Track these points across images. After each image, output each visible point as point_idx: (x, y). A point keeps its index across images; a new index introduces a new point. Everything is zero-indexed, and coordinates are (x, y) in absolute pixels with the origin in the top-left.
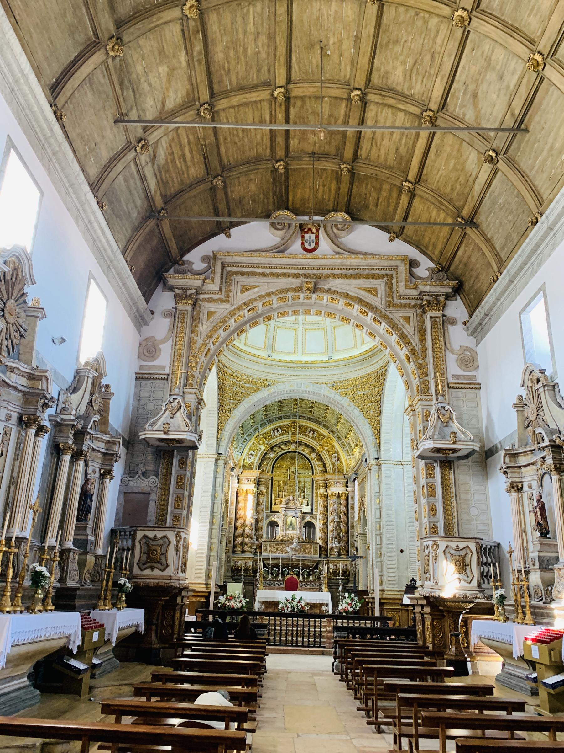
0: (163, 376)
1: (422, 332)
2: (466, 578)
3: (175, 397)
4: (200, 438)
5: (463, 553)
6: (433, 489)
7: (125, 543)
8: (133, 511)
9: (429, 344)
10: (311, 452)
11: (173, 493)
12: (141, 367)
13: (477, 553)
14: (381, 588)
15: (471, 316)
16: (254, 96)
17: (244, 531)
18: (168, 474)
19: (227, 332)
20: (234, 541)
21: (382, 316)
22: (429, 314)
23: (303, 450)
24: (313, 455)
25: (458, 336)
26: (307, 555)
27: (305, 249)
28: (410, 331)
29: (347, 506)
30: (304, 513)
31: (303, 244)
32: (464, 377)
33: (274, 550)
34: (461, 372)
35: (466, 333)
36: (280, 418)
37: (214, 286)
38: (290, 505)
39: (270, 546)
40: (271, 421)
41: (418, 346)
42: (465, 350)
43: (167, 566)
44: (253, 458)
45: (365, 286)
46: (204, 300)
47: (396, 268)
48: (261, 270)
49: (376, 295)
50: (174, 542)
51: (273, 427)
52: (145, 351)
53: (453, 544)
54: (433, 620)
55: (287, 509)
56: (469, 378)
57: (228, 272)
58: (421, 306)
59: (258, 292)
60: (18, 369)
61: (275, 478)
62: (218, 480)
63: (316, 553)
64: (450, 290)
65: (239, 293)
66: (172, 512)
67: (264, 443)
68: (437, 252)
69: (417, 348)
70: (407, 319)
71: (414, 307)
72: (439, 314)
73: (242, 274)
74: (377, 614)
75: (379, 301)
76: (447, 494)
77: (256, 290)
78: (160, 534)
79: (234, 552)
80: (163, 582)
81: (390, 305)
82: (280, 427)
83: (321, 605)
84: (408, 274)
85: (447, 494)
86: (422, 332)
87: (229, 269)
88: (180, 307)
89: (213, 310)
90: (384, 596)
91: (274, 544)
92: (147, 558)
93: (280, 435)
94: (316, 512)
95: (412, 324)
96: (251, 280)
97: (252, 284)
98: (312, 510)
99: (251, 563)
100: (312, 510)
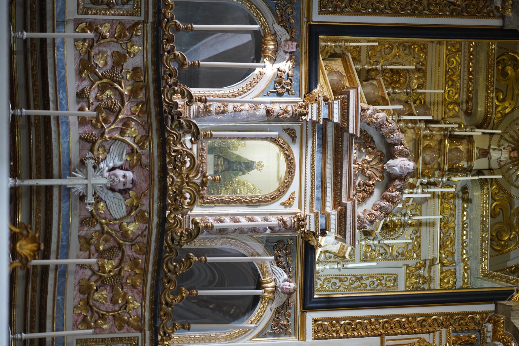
26: (72, 296)
30: (309, 250)
33: (102, 63)
38: (358, 157)
39: (125, 33)
55: (335, 139)
98: (330, 303)
100: (330, 303)
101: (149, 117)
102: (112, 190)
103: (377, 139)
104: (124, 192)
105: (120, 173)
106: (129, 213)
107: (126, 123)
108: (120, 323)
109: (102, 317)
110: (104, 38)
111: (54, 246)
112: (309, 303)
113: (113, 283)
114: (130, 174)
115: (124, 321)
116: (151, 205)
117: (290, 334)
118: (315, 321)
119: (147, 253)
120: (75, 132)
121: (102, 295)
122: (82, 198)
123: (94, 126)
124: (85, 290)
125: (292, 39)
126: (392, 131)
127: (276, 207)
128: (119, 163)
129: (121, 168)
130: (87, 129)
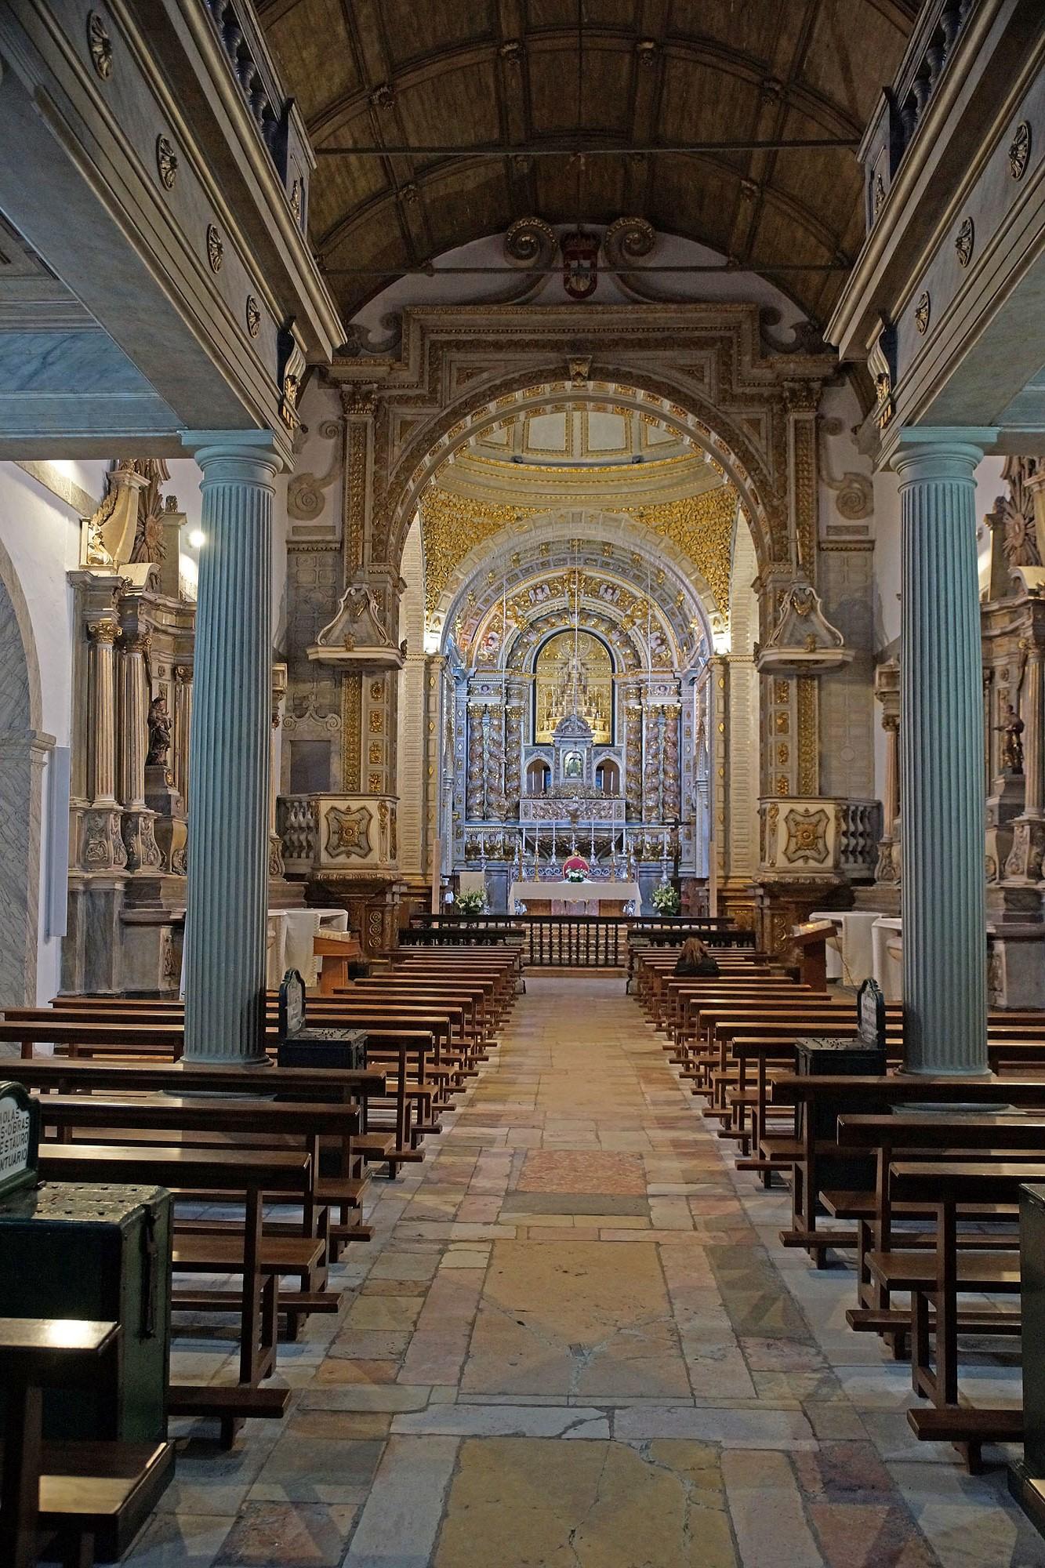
0: (333, 546)
1: (780, 448)
2: (816, 855)
3: (357, 586)
4: (403, 652)
5: (814, 820)
6: (785, 721)
7: (301, 817)
8: (307, 772)
9: (791, 470)
11: (367, 740)
12: (296, 530)
13: (837, 818)
14: (721, 873)
15: (865, 417)
16: (465, 59)
18: (355, 711)
19: (436, 456)
21: (710, 419)
22: (792, 417)
23: (594, 626)
25: (841, 454)
27: (572, 292)
28: (760, 445)
31: (567, 281)
32: (848, 530)
34: (843, 521)
35: (855, 448)
36: (545, 565)
37: (409, 375)
40: (528, 572)
41: (772, 478)
42: (851, 481)
43: (370, 850)
44: (495, 645)
45: (682, 362)
46: (391, 400)
47: (737, 328)
48: (491, 337)
49: (701, 380)
50: (377, 816)
51: (532, 582)
52: (299, 501)
53: (800, 807)
54: (773, 916)
56: (857, 530)
57: (433, 344)
58: (781, 399)
59: (489, 380)
60: (165, 606)
61: (541, 680)
62: (432, 699)
63: (619, 816)
64: (831, 371)
65: (454, 384)
66: (366, 767)
67: (516, 617)
68: (811, 295)
69: (771, 480)
70: (755, 424)
71: (767, 400)
72: (811, 416)
73: (459, 345)
74: (714, 914)
75: (705, 390)
76: (806, 729)
77: (485, 375)
78: (355, 805)
80: (368, 874)
81: (727, 397)
82: (546, 582)
83: (623, 903)
84: (758, 339)
85: (806, 729)
86: (780, 448)
87: (434, 337)
88: (352, 417)
89: (409, 418)
90: (730, 886)
91: (541, 803)
92: (340, 839)
93: (547, 598)
95: (763, 435)
96: (474, 358)
97: (477, 365)
99: (500, 837)
112: (613, 745)
113: (599, 811)
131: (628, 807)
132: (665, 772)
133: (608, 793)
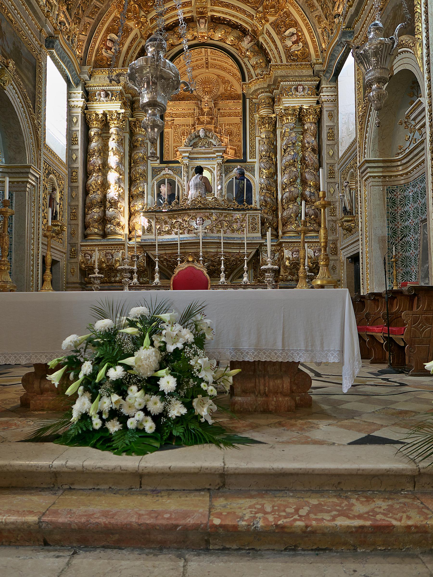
10: (240, 39)
17: (105, 196)
20: (85, 215)
24: (246, 43)
26: (235, 235)
29: (318, 135)
30: (228, 161)
63: (254, 229)
79: (85, 236)
94: (253, 156)
101: (182, 213)
102: (203, 224)
103: (194, 141)
104: (203, 220)
105: (198, 222)
106: (210, 219)
107: (184, 220)
108: (243, 220)
109: (242, 226)
110: (160, 227)
111: (219, 241)
112: (245, 161)
114: (198, 219)
115: (243, 219)
116: (207, 212)
117: (254, 166)
118: (250, 158)
119: (222, 213)
120: (186, 235)
121: (235, 226)
122: (205, 233)
123: (185, 230)
124: (233, 231)
125: (164, 170)
126: (191, 136)
127: (215, 172)
128: (195, 222)
129: (196, 222)
130: (186, 232)
131: (263, 224)
132: (304, 182)
133: (241, 202)
